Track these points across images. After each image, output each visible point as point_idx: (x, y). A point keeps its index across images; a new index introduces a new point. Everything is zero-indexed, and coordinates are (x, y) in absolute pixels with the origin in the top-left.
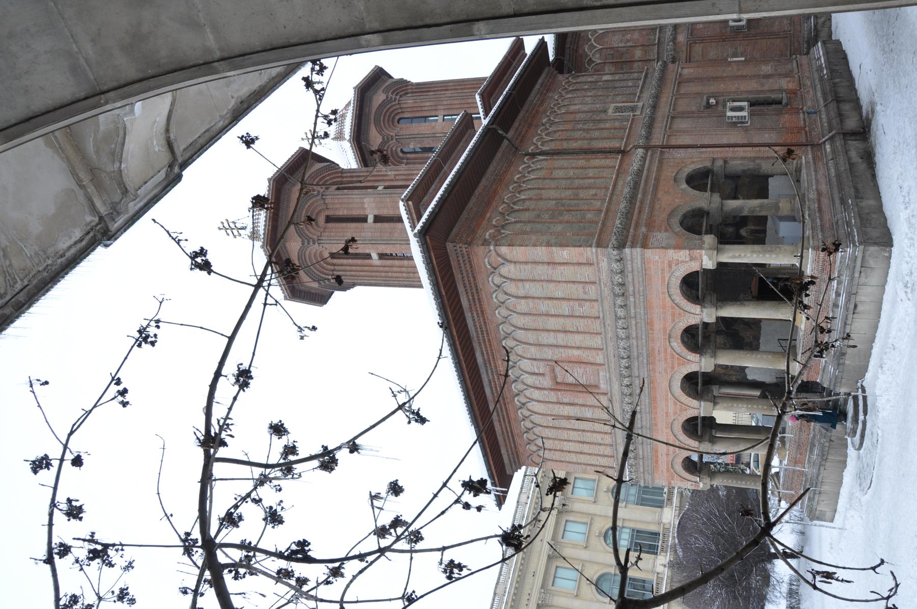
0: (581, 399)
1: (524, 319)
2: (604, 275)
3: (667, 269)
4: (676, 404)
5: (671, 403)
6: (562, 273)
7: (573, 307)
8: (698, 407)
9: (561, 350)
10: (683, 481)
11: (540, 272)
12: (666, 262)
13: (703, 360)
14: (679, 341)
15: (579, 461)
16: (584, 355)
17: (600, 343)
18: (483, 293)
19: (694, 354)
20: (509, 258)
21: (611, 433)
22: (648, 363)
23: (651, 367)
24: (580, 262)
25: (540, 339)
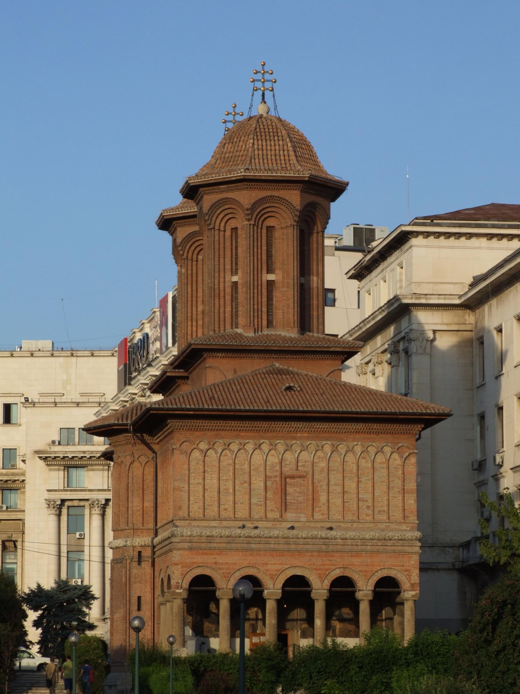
0: (272, 496)
1: (352, 463)
2: (396, 527)
3: (403, 568)
4: (277, 571)
5: (279, 567)
6: (395, 497)
7: (366, 501)
8: (275, 588)
9: (325, 487)
10: (182, 575)
11: (395, 482)
12: (409, 568)
13: (325, 591)
14: (341, 575)
15: (191, 486)
16: (320, 504)
17: (334, 518)
18: (375, 436)
19: (329, 585)
20: (407, 461)
21: (235, 517)
22: (319, 551)
23: (316, 554)
24: (406, 511)
25: (333, 472)
